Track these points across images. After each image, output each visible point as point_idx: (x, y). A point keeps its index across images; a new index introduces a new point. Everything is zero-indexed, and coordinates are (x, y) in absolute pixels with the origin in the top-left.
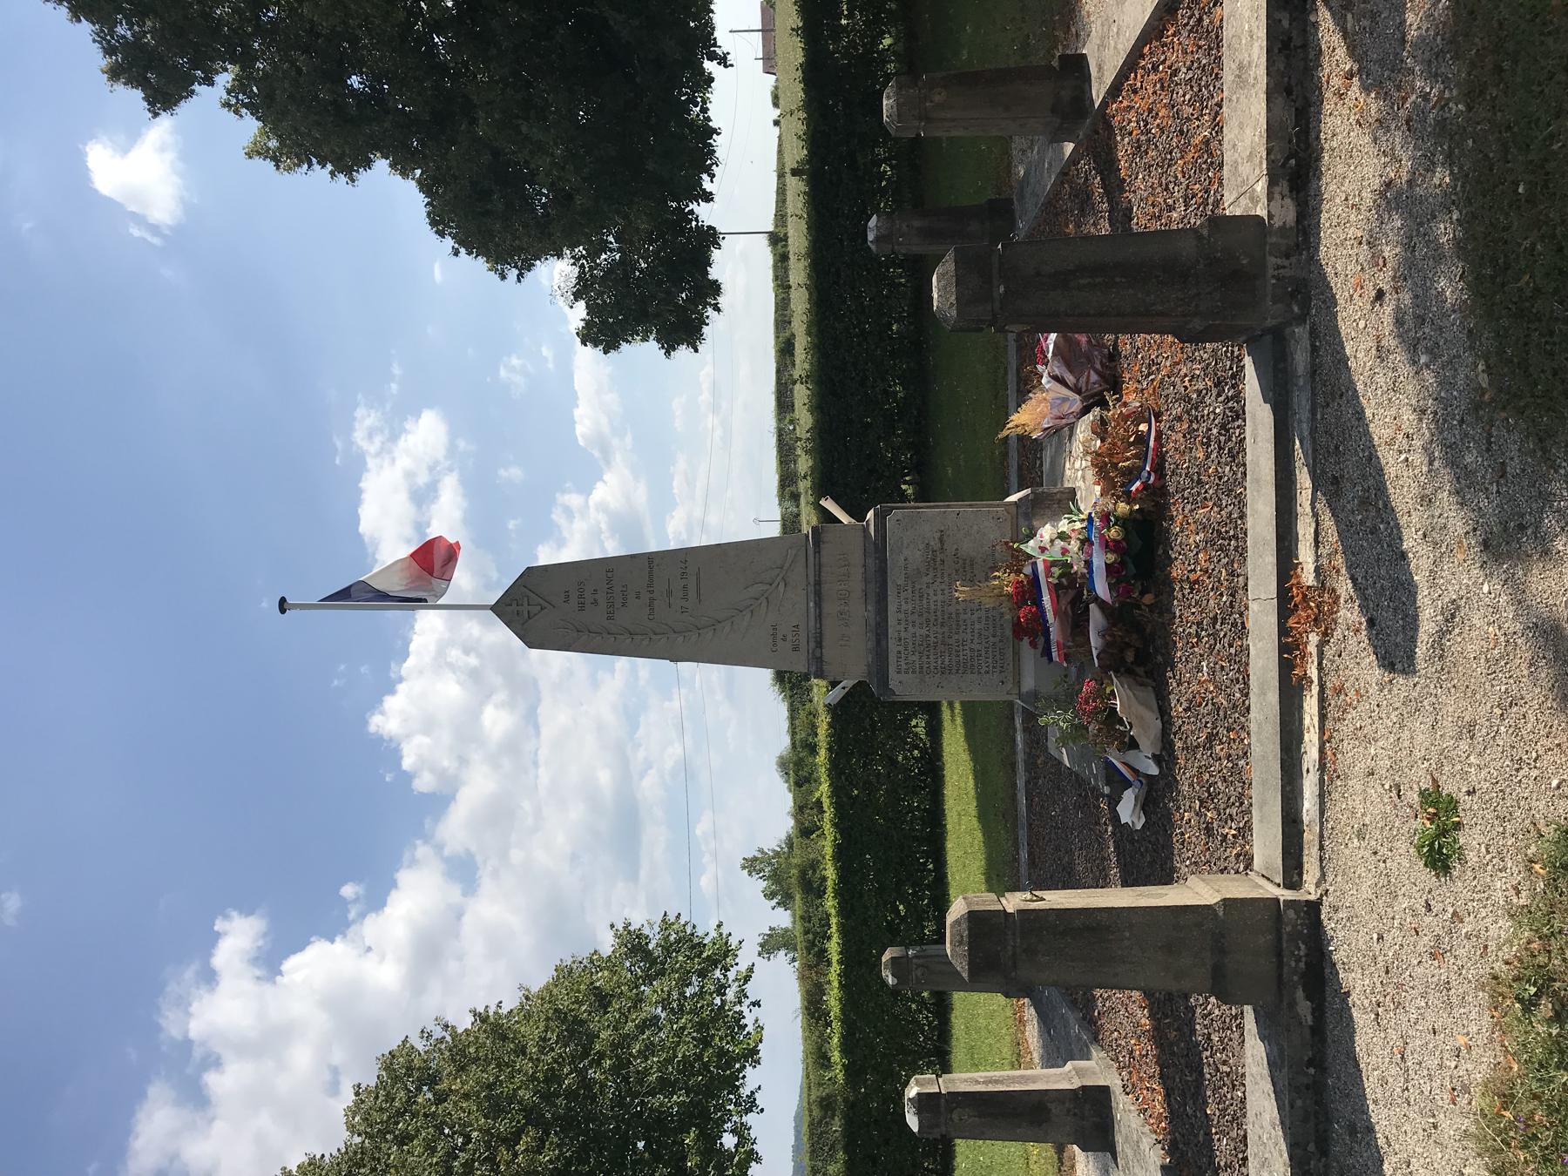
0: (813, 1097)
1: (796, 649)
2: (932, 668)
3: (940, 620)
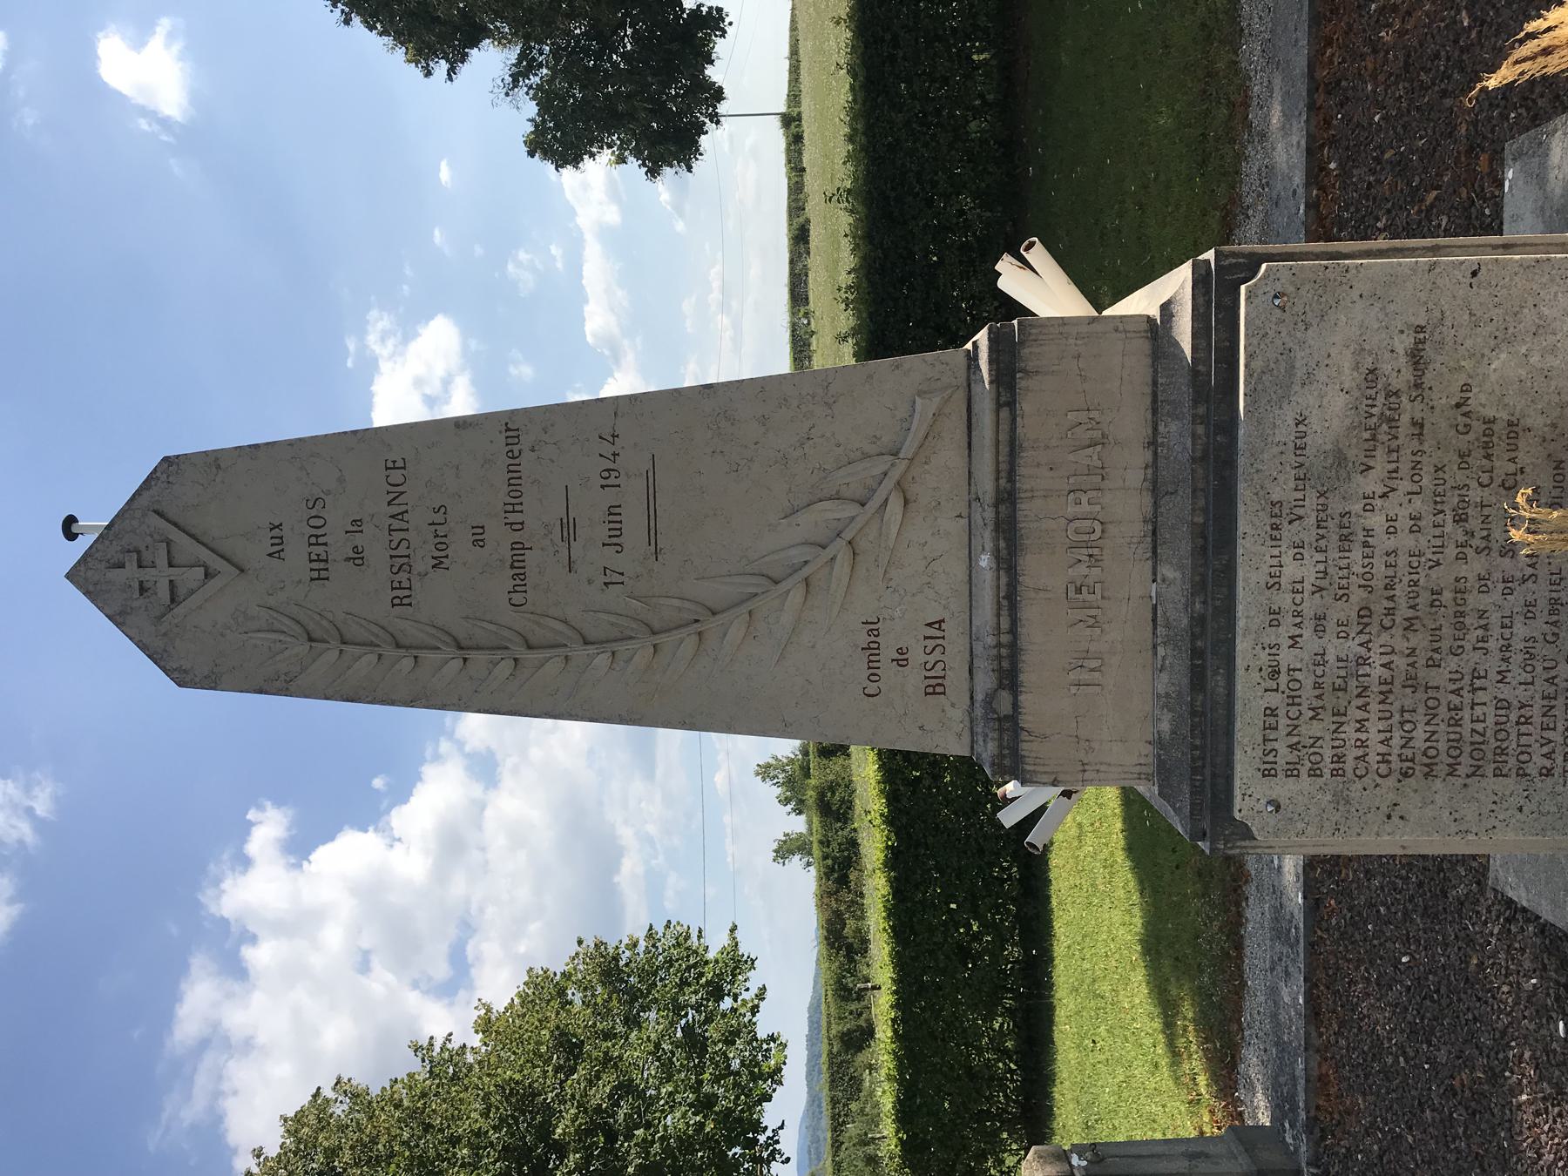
0: (833, 1032)
1: (935, 689)
2: (1373, 758)
3: (1403, 612)
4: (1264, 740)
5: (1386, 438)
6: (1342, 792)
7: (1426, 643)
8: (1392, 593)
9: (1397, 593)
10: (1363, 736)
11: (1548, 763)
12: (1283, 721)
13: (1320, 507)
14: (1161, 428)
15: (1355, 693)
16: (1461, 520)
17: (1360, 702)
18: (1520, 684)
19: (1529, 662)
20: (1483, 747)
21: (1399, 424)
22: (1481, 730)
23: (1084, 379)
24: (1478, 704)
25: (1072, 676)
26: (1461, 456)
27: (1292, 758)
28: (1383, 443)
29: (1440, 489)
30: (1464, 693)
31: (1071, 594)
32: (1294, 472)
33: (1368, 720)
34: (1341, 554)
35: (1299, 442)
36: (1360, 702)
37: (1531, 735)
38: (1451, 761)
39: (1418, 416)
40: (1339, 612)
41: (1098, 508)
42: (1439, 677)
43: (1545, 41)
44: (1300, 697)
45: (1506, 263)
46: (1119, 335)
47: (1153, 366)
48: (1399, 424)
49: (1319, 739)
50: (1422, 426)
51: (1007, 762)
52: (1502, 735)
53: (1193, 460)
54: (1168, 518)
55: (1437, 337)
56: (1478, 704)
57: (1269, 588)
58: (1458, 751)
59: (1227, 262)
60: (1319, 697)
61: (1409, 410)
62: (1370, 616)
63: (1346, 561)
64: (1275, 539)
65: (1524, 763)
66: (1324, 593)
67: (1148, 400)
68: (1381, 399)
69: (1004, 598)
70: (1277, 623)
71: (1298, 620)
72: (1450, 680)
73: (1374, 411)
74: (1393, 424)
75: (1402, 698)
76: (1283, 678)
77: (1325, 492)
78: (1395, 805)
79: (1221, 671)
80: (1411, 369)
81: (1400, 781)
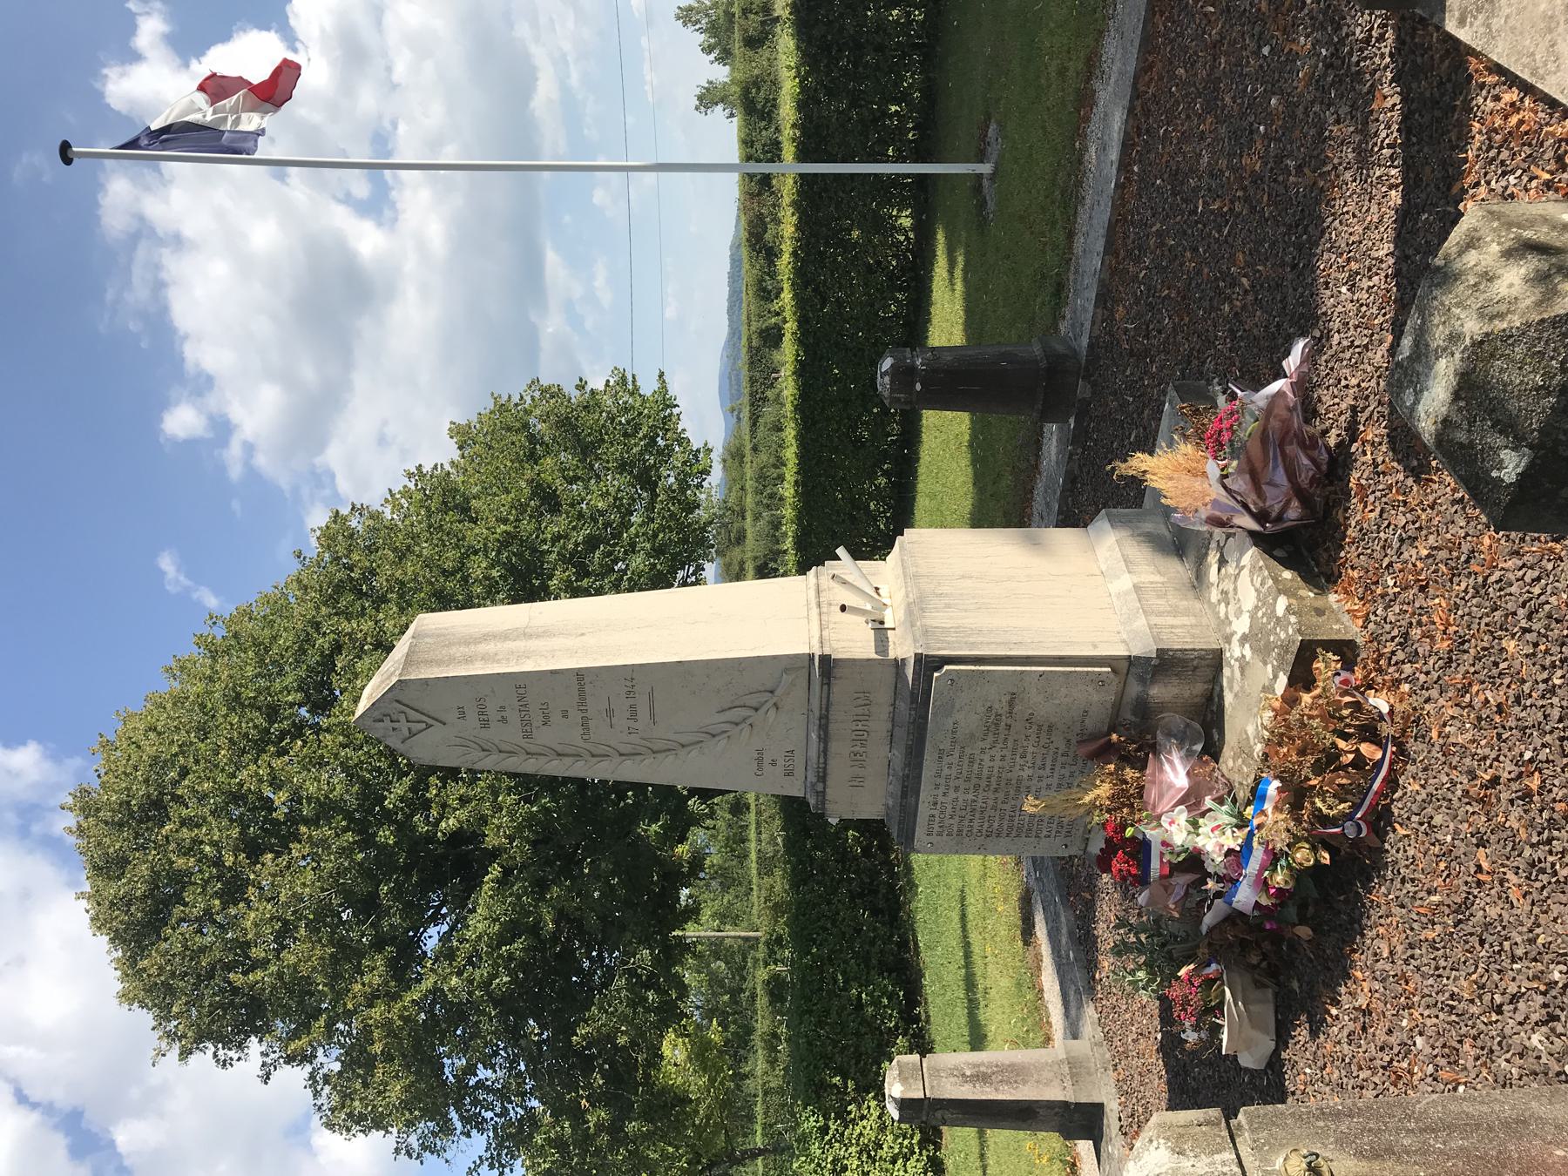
1: (789, 774)
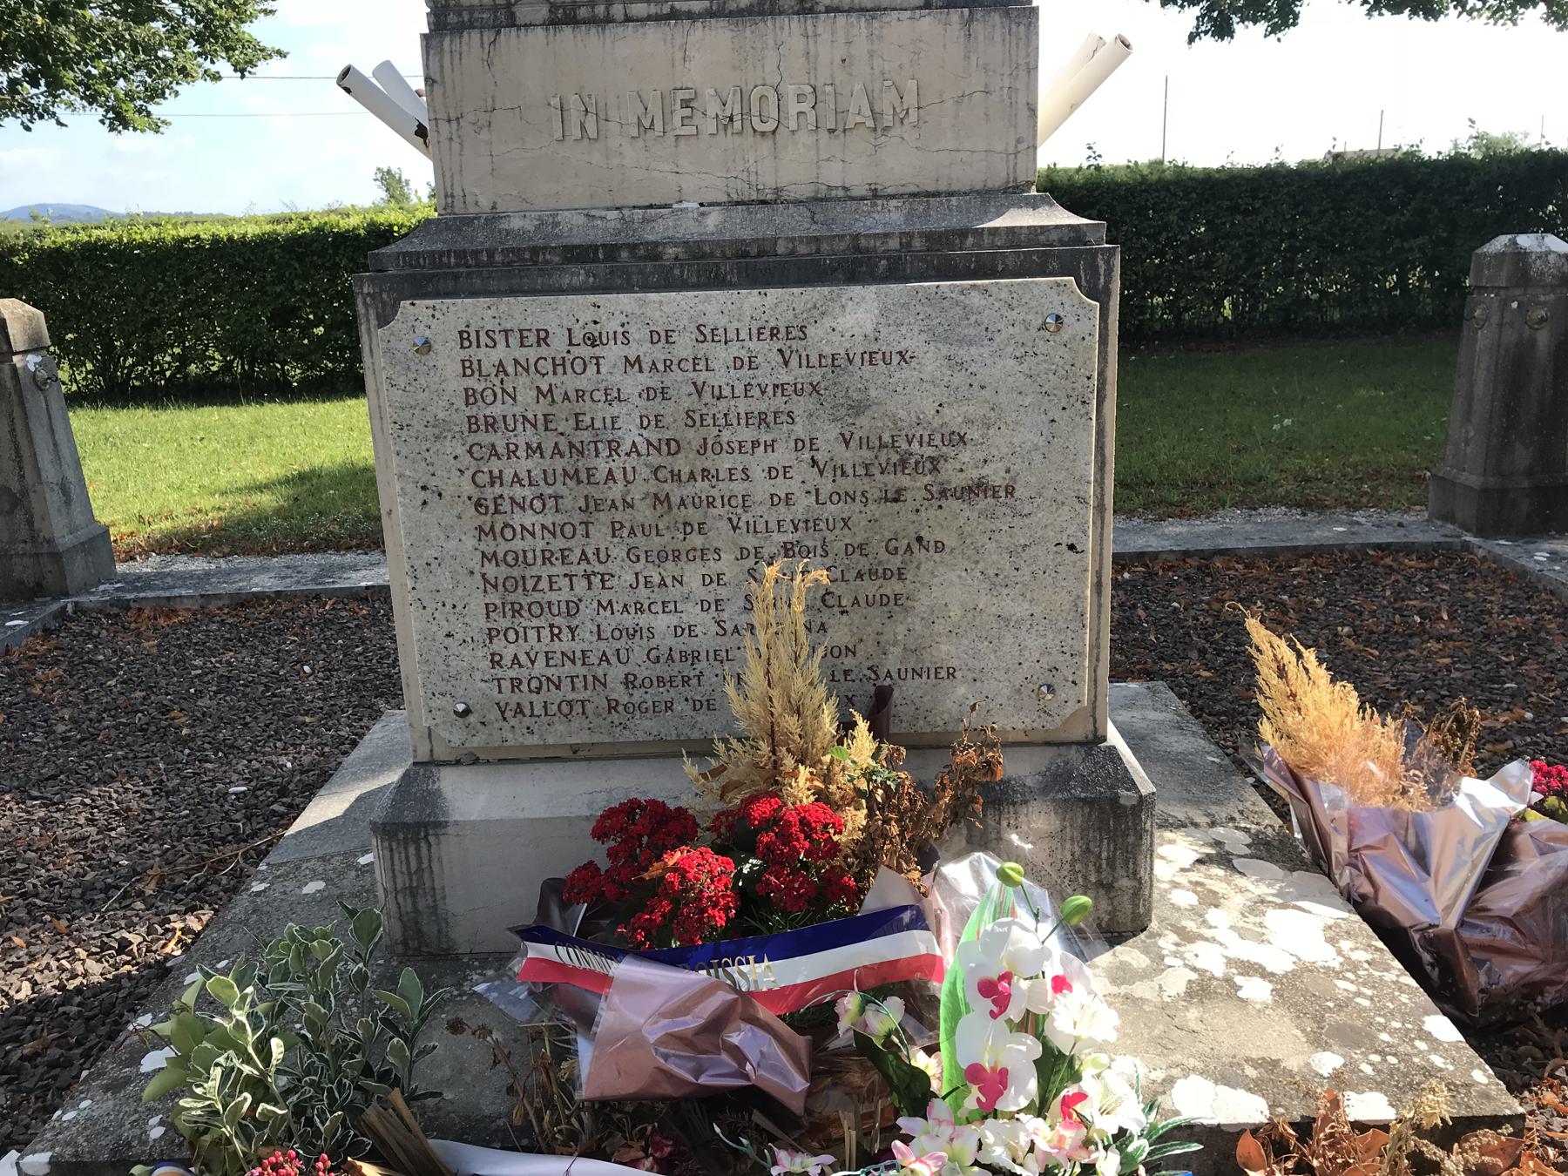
2: (495, 465)
3: (676, 492)
4: (506, 332)
5: (883, 460)
6: (449, 431)
7: (640, 518)
8: (699, 479)
9: (699, 483)
10: (521, 453)
11: (507, 661)
12: (532, 353)
13: (799, 386)
14: (894, 203)
15: (576, 441)
16: (787, 550)
17: (564, 447)
18: (598, 626)
19: (624, 633)
20: (520, 589)
21: (899, 474)
22: (540, 587)
23: (959, 101)
24: (571, 581)
25: (573, 102)
26: (861, 546)
27: (487, 367)
28: (876, 457)
29: (822, 525)
30: (584, 565)
31: (681, 95)
32: (842, 352)
33: (542, 456)
34: (743, 415)
35: (879, 356)
36: (564, 447)
37: (539, 640)
38: (500, 555)
39: (908, 495)
40: (672, 411)
41: (793, 125)
42: (600, 536)
43: (1292, 670)
44: (565, 373)
45: (1079, 580)
46: (1012, 143)
47: (972, 191)
48: (899, 474)
49: (514, 399)
50: (896, 500)
51: (452, 18)
52: (536, 609)
53: (856, 237)
54: (782, 215)
55: (1001, 510)
56: (571, 581)
57: (698, 328)
58: (513, 563)
59: (1101, 263)
60: (566, 397)
61: (914, 484)
62: (669, 454)
63: (735, 422)
64: (759, 334)
65: (505, 635)
66: (695, 396)
67: (931, 188)
68: (929, 451)
69: (672, 7)
70: (655, 340)
71: (661, 367)
72: (598, 549)
73: (915, 446)
74: (899, 468)
75: (572, 496)
76: (586, 351)
77: (818, 392)
78: (440, 495)
79: (591, 279)
80: (964, 484)
81: (470, 498)
